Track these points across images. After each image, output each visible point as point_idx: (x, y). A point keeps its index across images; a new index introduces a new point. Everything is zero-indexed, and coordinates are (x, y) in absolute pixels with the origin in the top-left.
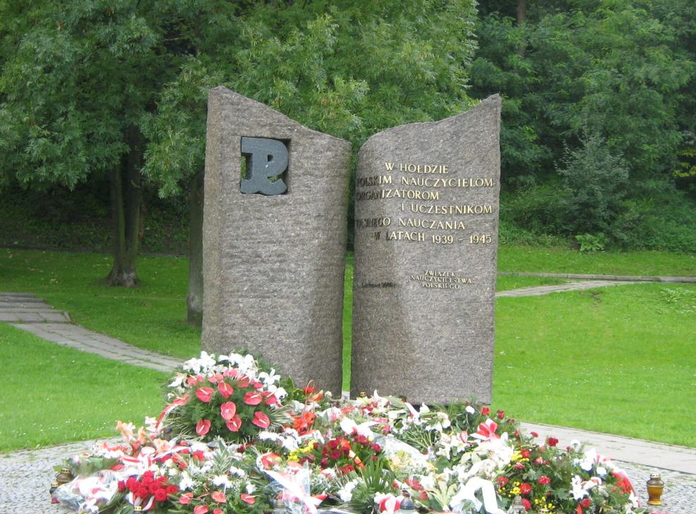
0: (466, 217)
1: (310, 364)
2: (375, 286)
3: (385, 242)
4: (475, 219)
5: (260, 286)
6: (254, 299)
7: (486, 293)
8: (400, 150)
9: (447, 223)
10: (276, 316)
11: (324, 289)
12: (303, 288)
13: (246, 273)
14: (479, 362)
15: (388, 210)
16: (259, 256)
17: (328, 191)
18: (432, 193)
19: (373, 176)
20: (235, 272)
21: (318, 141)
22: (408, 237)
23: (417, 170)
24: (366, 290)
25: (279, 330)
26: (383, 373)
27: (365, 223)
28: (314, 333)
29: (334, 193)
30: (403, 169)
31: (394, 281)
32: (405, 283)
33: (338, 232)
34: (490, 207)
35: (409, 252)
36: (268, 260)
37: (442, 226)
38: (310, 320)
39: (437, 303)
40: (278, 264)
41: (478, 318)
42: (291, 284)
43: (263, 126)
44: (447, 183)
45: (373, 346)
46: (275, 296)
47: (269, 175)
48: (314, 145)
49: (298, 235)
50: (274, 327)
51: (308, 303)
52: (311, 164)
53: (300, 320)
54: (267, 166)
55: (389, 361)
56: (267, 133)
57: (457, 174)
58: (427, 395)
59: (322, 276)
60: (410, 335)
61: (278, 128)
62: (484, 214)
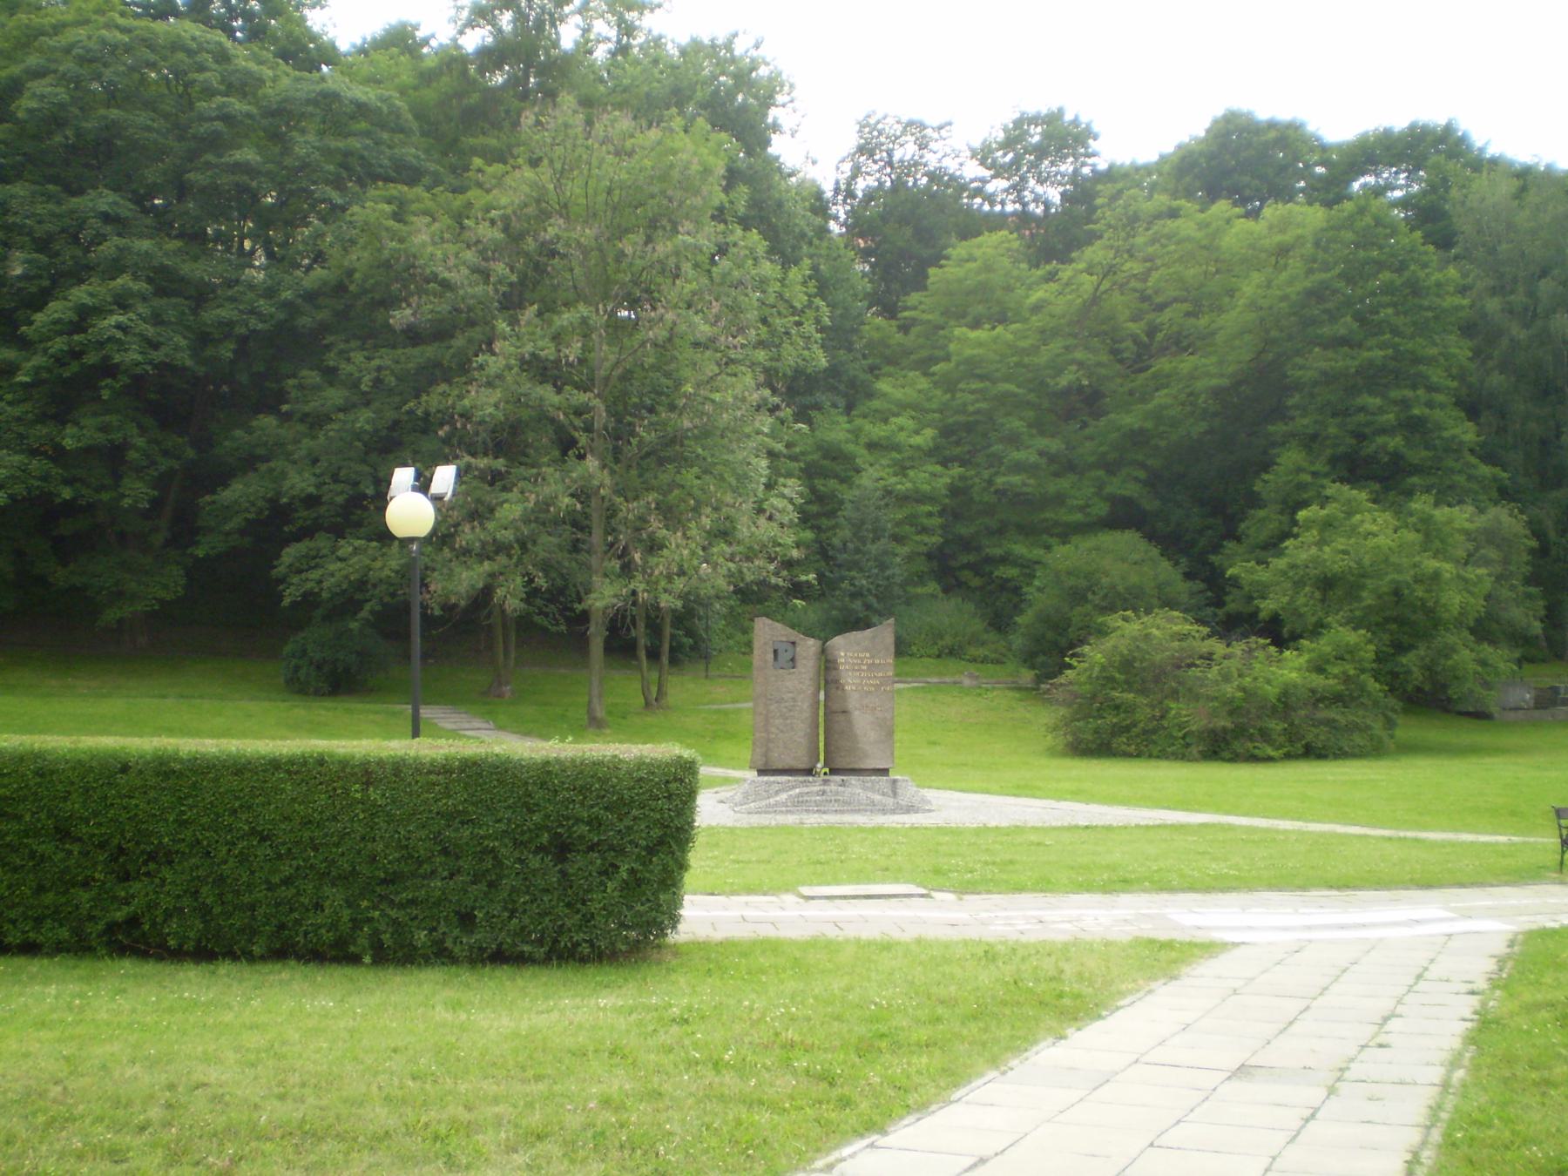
20: (772, 707)
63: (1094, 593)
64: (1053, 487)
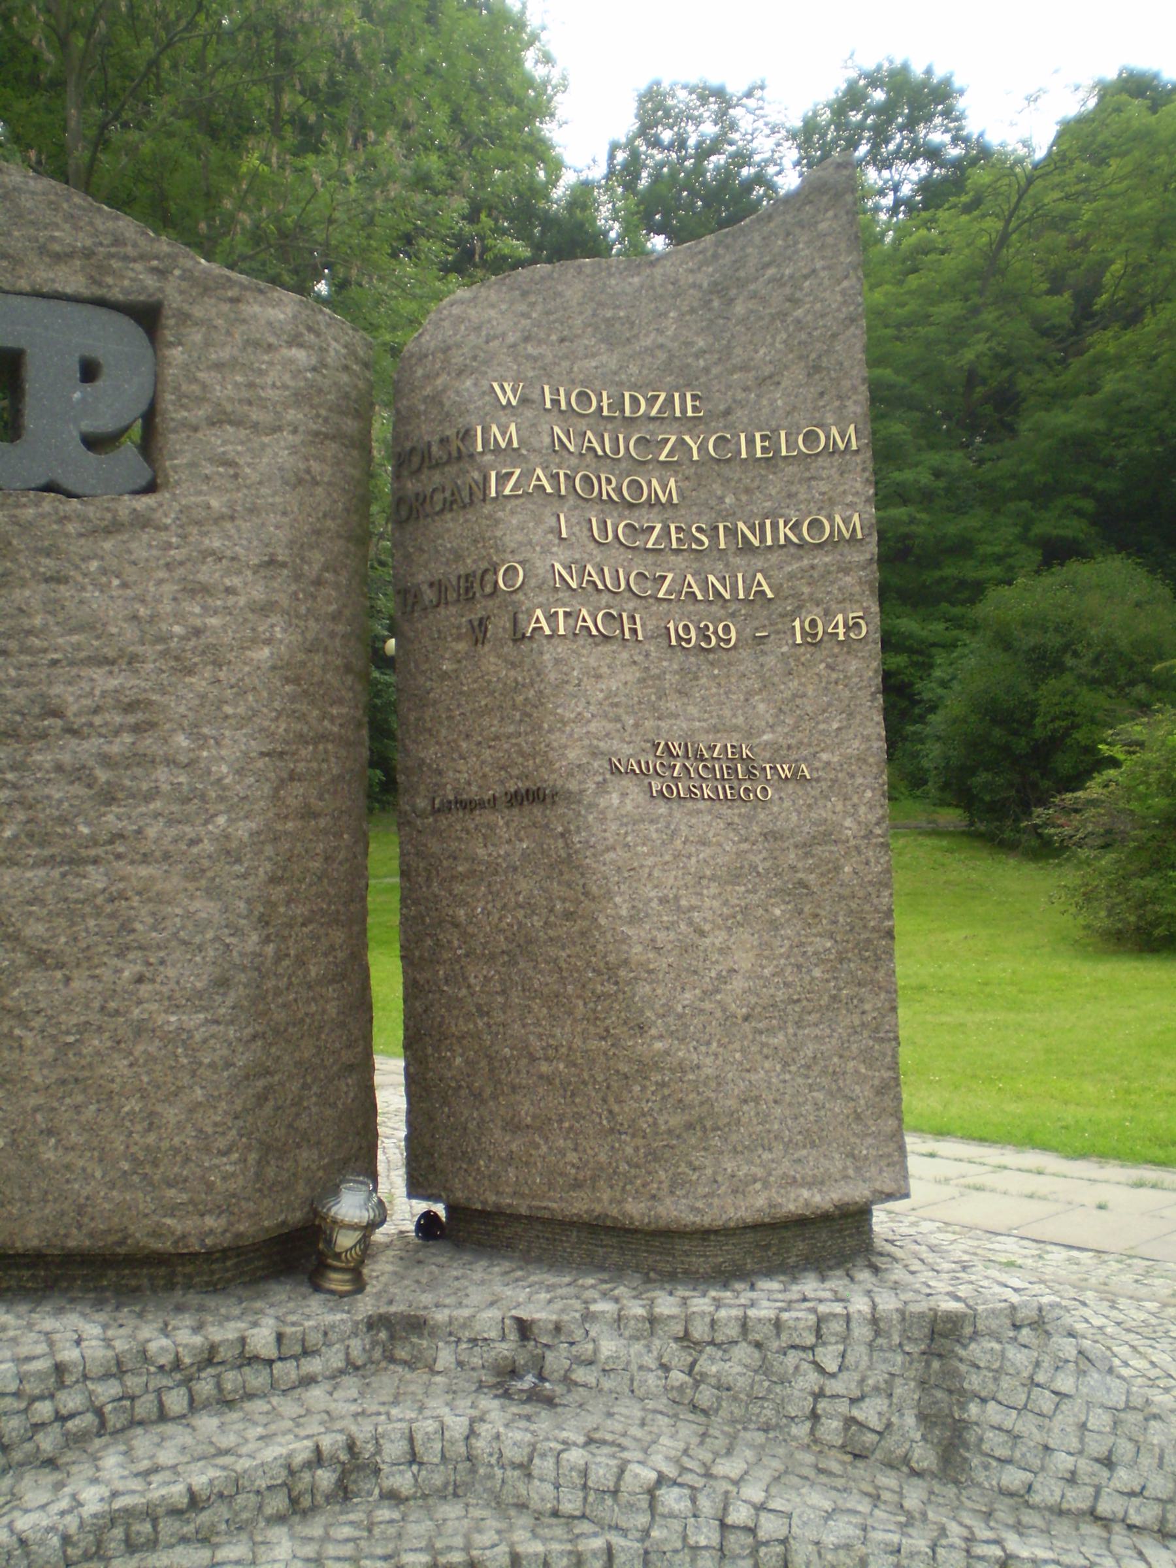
0: (774, 558)
1: (262, 1098)
2: (481, 804)
3: (509, 648)
4: (806, 562)
5: (63, 820)
6: (41, 872)
7: (862, 810)
8: (540, 342)
9: (711, 578)
10: (126, 927)
11: (299, 824)
12: (221, 820)
13: (10, 776)
14: (854, 1047)
15: (511, 541)
16: (57, 713)
17: (300, 481)
18: (654, 482)
19: (450, 432)
21: (257, 309)
22: (590, 624)
23: (600, 408)
24: (444, 822)
25: (140, 979)
26: (526, 1110)
27: (429, 595)
28: (270, 984)
29: (319, 490)
30: (556, 402)
31: (550, 779)
32: (591, 786)
33: (341, 628)
34: (856, 518)
35: (598, 677)
36: (91, 725)
37: (696, 589)
38: (255, 938)
39: (706, 853)
40: (127, 738)
41: (842, 897)
42: (175, 808)
43: (59, 258)
44: (702, 448)
45: (482, 1012)
46: (119, 857)
47: (87, 426)
48: (244, 321)
49: (197, 632)
50: (118, 971)
51: (244, 877)
52: (237, 385)
53: (217, 939)
54: (77, 395)
55: (544, 1068)
56: (72, 280)
57: (732, 418)
58: (701, 1190)
59: (293, 777)
60: (622, 973)
61: (115, 264)
62: (832, 544)
63: (1076, 654)
64: (953, 528)
